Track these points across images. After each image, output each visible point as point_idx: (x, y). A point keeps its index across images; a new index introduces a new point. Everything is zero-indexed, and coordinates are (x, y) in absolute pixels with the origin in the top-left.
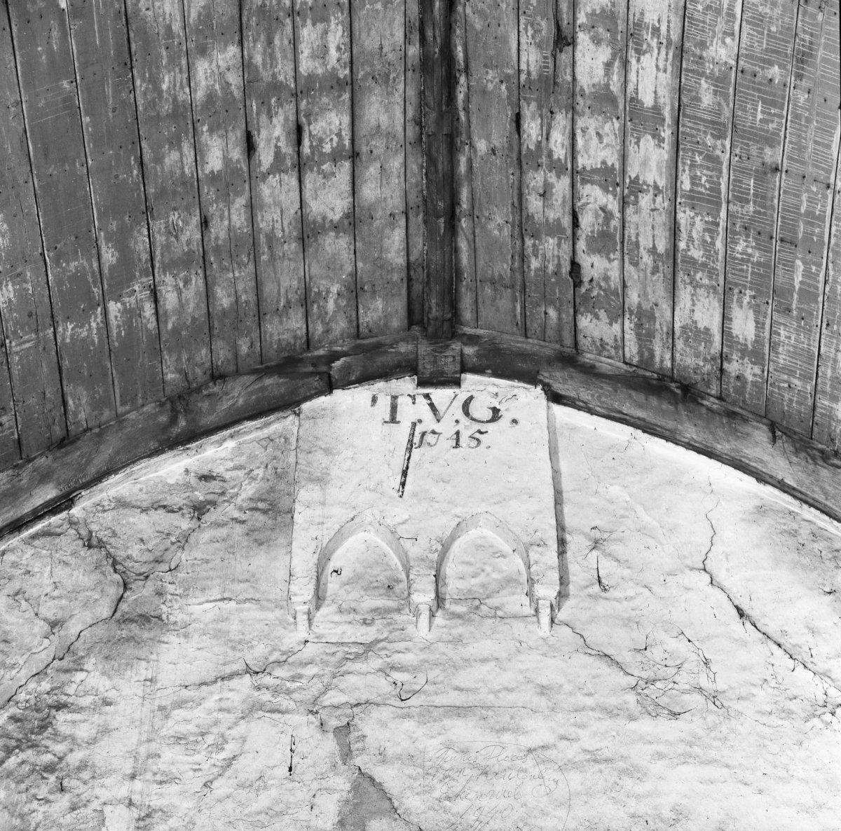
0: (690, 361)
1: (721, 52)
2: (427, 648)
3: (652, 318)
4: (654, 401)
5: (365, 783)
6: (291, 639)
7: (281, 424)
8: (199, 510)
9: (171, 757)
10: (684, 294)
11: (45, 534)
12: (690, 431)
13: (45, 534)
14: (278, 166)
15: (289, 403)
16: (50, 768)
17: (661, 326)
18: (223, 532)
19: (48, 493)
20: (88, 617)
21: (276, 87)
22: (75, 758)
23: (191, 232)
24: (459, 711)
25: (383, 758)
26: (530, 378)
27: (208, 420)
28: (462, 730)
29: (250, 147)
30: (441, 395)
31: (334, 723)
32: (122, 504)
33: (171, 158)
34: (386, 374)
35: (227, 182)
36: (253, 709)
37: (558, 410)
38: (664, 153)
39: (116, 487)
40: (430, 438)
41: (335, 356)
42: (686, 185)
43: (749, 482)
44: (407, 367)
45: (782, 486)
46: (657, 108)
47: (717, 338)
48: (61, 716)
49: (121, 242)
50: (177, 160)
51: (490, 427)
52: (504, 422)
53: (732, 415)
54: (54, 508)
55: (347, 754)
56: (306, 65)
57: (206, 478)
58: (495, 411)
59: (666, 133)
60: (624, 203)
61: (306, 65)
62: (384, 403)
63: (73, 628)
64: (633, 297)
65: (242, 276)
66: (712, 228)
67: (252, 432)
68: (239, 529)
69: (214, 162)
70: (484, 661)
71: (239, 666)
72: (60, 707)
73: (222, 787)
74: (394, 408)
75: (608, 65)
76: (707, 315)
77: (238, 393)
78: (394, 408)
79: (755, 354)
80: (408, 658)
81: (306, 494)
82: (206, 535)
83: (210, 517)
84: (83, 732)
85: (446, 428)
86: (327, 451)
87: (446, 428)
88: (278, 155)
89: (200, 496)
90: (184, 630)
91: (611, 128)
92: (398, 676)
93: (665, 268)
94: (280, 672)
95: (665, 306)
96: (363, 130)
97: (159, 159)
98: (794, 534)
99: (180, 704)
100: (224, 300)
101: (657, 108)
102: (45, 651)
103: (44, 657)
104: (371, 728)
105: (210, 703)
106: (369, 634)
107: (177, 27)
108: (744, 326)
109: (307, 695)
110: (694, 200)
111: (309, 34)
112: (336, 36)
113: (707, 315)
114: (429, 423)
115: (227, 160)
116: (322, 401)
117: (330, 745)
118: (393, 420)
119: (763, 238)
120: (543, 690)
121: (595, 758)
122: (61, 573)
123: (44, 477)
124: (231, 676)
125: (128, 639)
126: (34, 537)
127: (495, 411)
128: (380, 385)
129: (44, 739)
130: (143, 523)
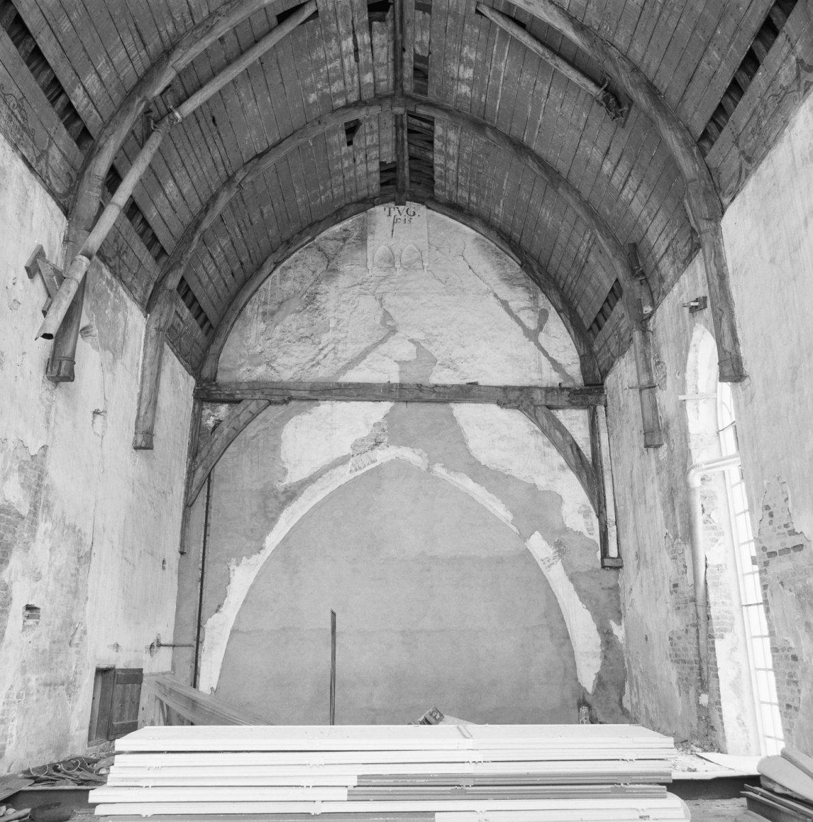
0: (461, 202)
1: (468, 149)
2: (399, 277)
3: (452, 192)
4: (452, 211)
5: (386, 312)
6: (367, 275)
7: (361, 215)
8: (344, 240)
9: (343, 306)
10: (460, 191)
11: (309, 247)
12: (461, 219)
13: (309, 247)
14: (361, 162)
15: (365, 210)
16: (317, 309)
17: (454, 195)
18: (350, 246)
19: (309, 238)
20: (321, 270)
21: (361, 148)
22: (322, 307)
23: (340, 179)
24: (406, 294)
25: (390, 306)
26: (423, 203)
27: (345, 217)
28: (406, 299)
29: (355, 160)
30: (401, 208)
31: (378, 298)
32: (326, 238)
33: (336, 167)
34: (387, 202)
35: (348, 169)
36: (360, 294)
37: (429, 210)
38: (455, 164)
39: (324, 234)
40: (399, 221)
41: (375, 198)
42: (460, 171)
43: (473, 232)
44: (393, 200)
45: (482, 234)
46: (453, 156)
47: (467, 200)
48: (318, 296)
49: (324, 185)
50: (337, 167)
51: (412, 217)
52: (416, 216)
53: (471, 215)
54: (310, 241)
55: (382, 305)
56: (368, 143)
57: (345, 230)
58: (414, 212)
59: (456, 161)
60: (446, 171)
61: (368, 143)
62: (387, 209)
63: (318, 273)
64: (448, 188)
65: (353, 185)
66: (466, 180)
67: (355, 217)
68: (354, 245)
69: (346, 165)
70: (412, 281)
71: (356, 283)
72: (317, 293)
73: (355, 314)
74: (390, 212)
75: (442, 146)
76: (466, 195)
77: (352, 209)
78: (390, 212)
79: (476, 205)
80: (394, 280)
81: (370, 237)
82: (346, 247)
83: (347, 242)
84: (323, 300)
85: (402, 217)
86: (374, 225)
87: (402, 217)
88: (361, 161)
89: (344, 236)
90: (343, 273)
91: (442, 157)
92: (391, 285)
93: (455, 185)
94: (366, 284)
95: (455, 191)
96: (381, 153)
97: (333, 168)
98: (483, 246)
99: (344, 293)
100: (348, 190)
101: (453, 156)
102: (312, 279)
103: (312, 281)
104: (388, 299)
105: (351, 292)
106: (385, 274)
107: (337, 142)
108: (474, 198)
109: (372, 290)
110: (462, 174)
111: (369, 138)
112: (376, 136)
113: (466, 195)
114: (399, 216)
115: (349, 164)
116: (372, 209)
117: (378, 303)
118: (390, 215)
119: (478, 185)
120: (425, 289)
121: (437, 306)
122: (314, 258)
123: (308, 234)
124: (355, 285)
125: (331, 276)
126: (306, 248)
127: (414, 212)
128: (386, 204)
129: (314, 302)
130: (331, 244)
